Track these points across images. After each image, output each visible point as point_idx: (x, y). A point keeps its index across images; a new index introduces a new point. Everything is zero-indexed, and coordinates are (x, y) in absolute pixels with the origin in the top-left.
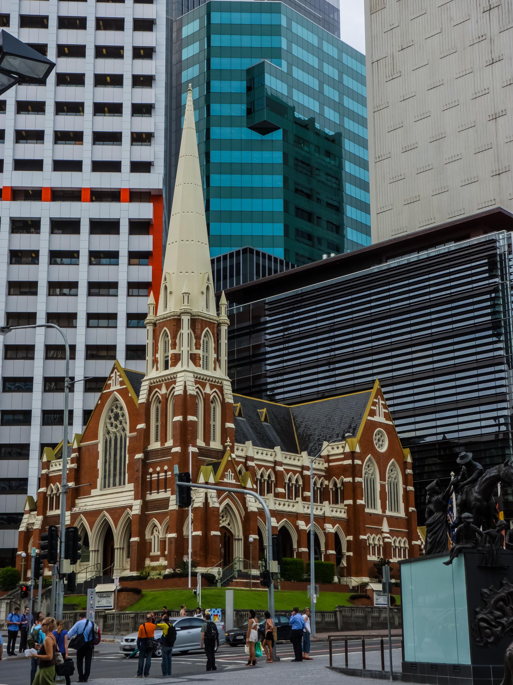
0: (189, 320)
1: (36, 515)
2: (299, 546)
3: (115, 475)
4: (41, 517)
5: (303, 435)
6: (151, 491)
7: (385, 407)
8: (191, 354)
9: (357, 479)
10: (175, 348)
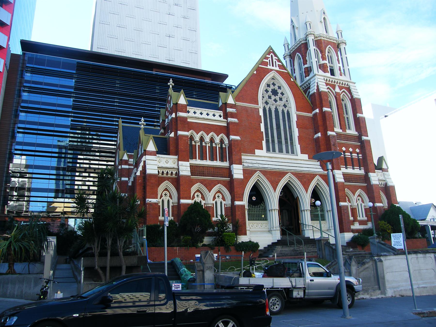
3: (280, 142)
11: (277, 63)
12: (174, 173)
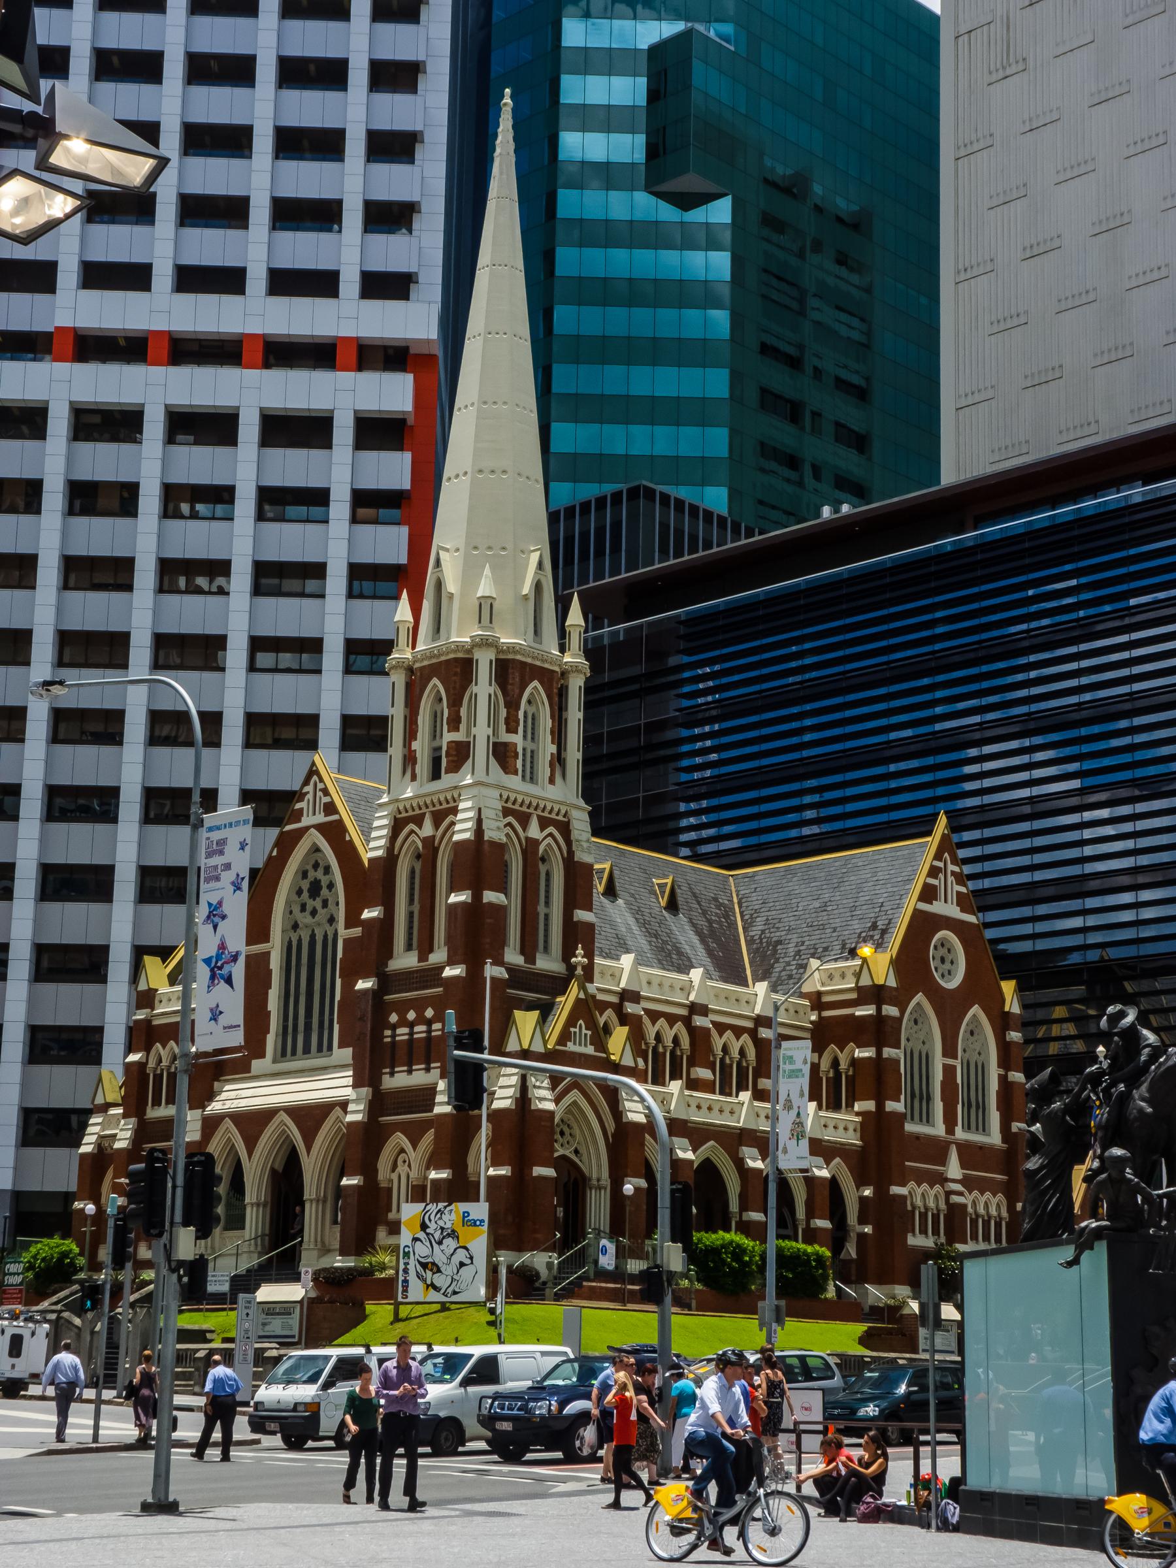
0: (491, 661)
1: (121, 1117)
2: (744, 1207)
4: (132, 1123)
5: (761, 942)
6: (393, 1067)
7: (960, 879)
8: (495, 744)
9: (888, 1052)
10: (457, 729)
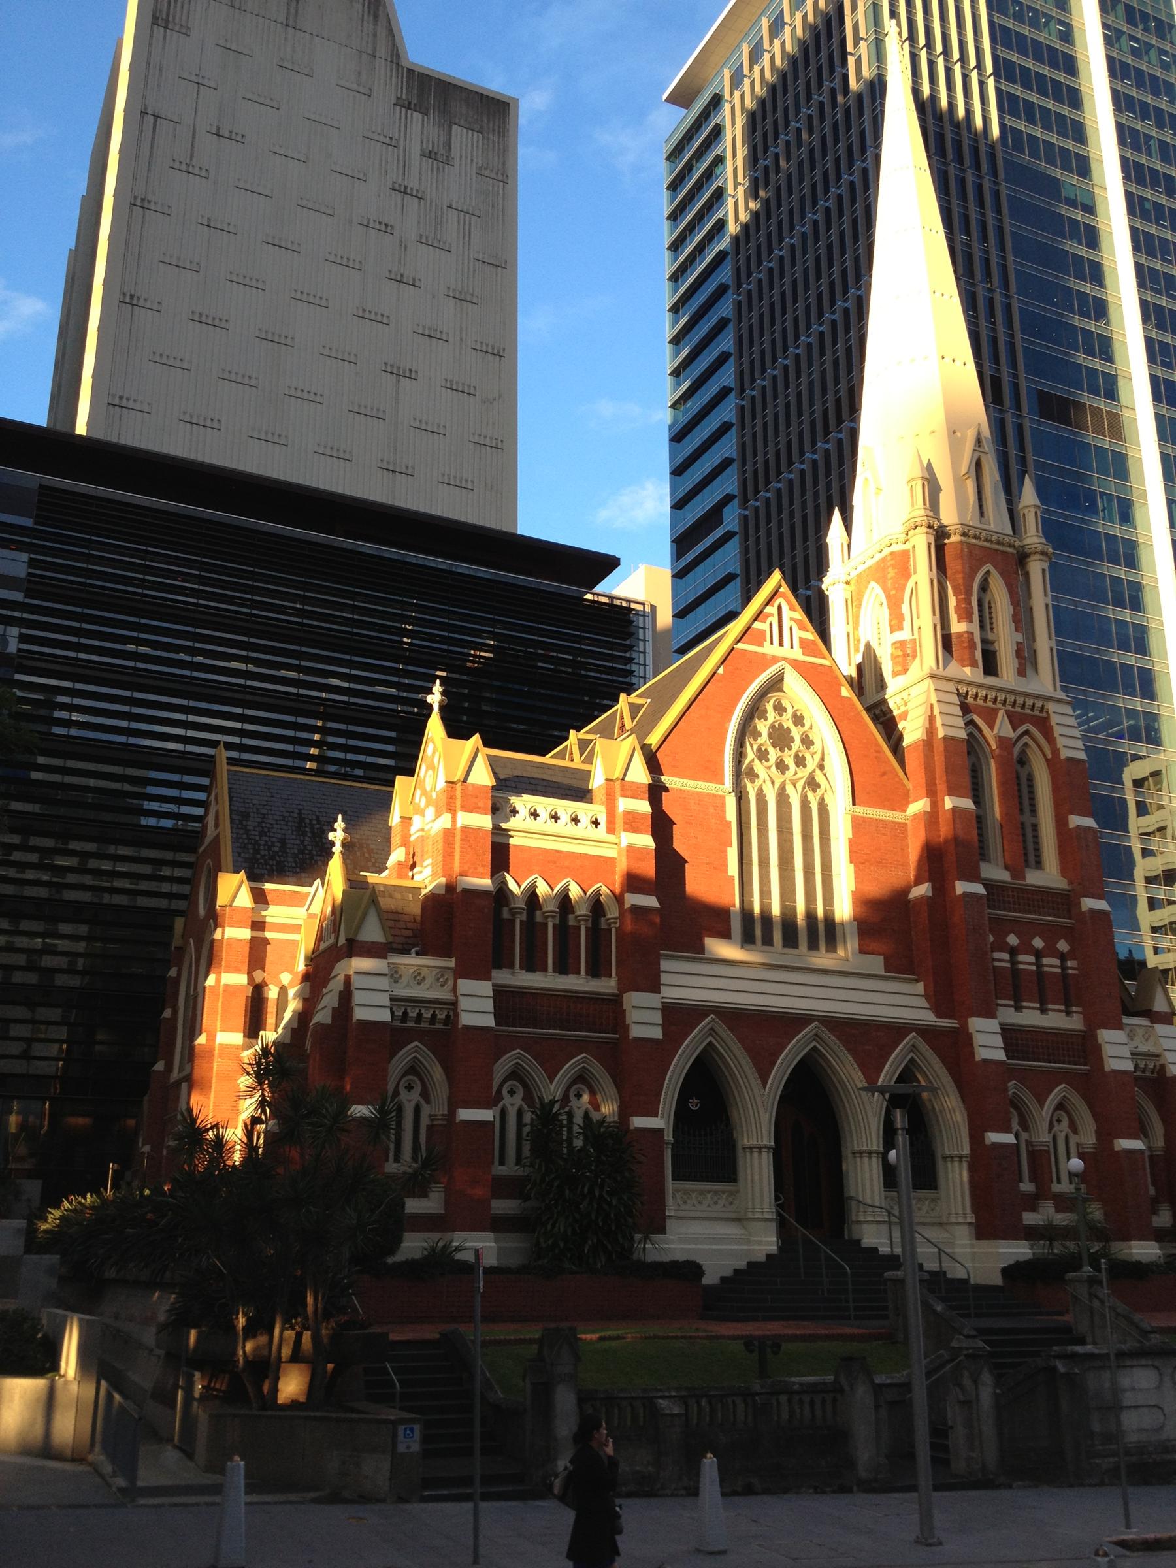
11: (798, 633)
12: (441, 1016)
